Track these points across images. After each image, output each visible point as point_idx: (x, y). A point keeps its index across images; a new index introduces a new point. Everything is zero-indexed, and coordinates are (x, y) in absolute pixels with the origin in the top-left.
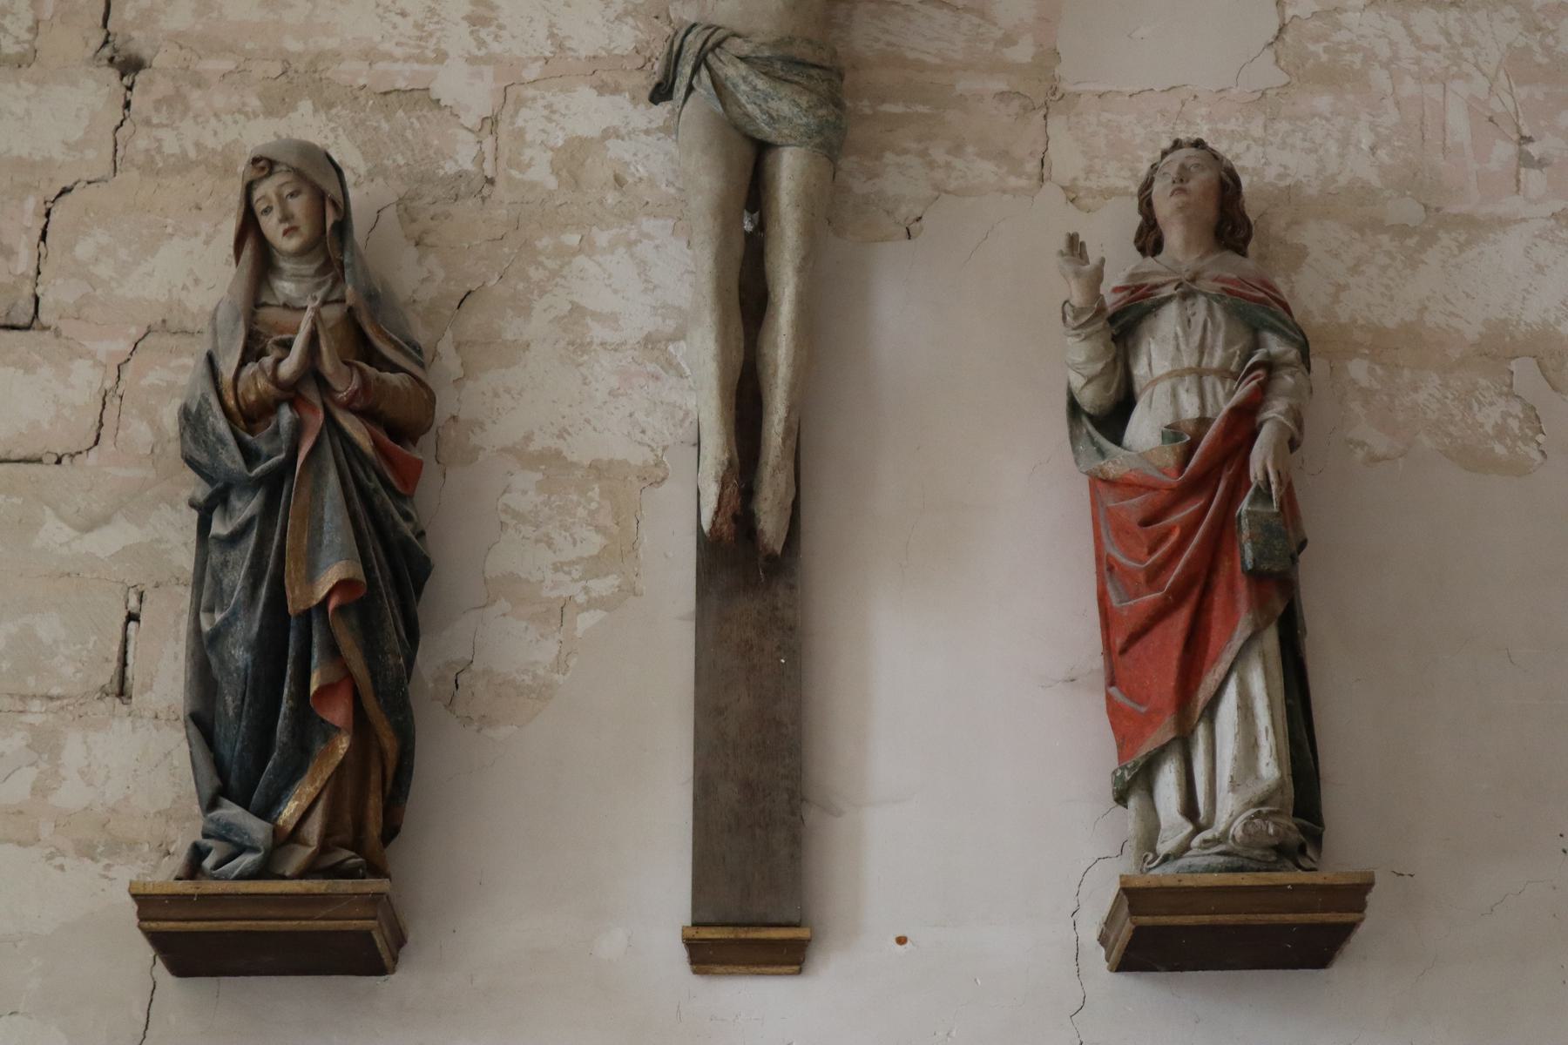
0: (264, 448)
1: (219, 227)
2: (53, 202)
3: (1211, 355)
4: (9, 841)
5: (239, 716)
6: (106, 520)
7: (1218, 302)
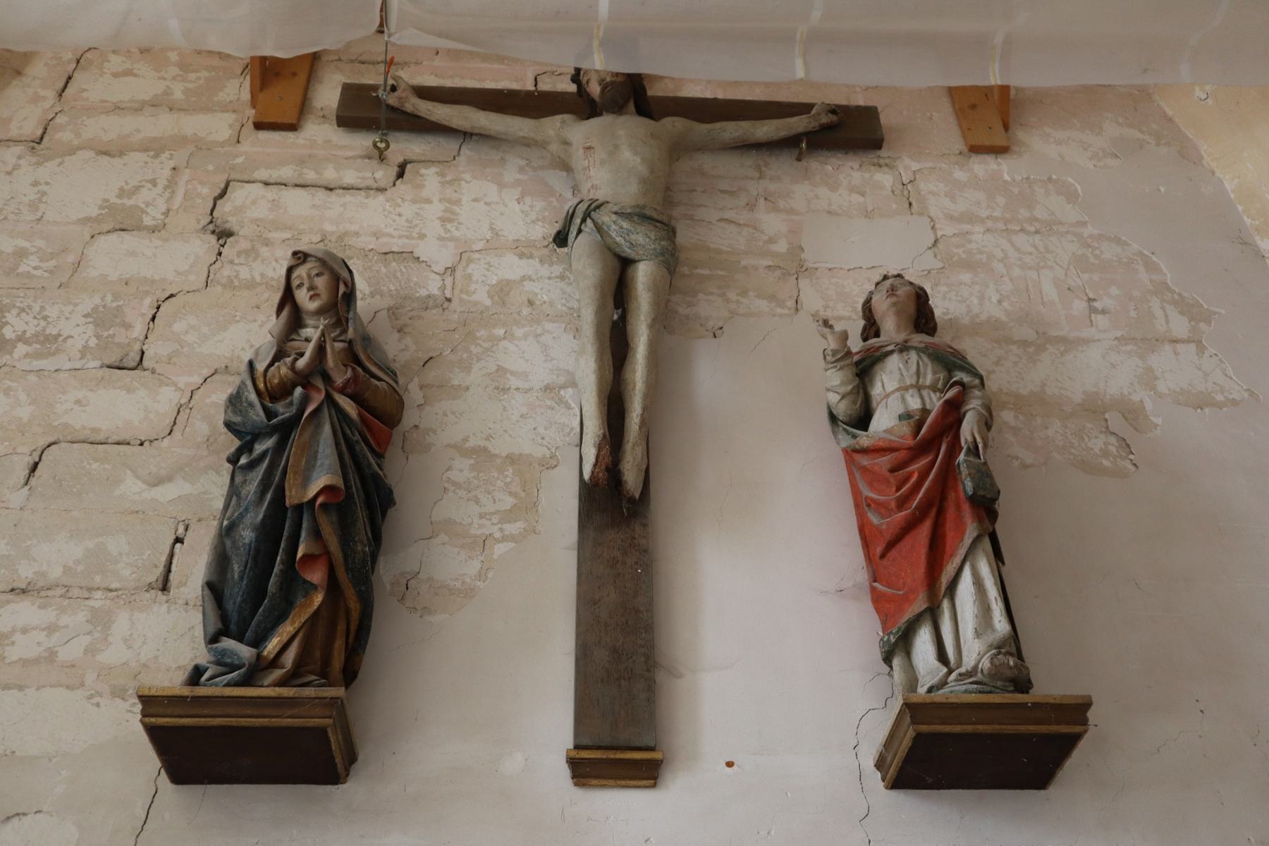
0: (281, 410)
1: (270, 318)
2: (163, 301)
3: (925, 378)
4: (61, 685)
5: (241, 578)
6: (169, 479)
7: (925, 353)
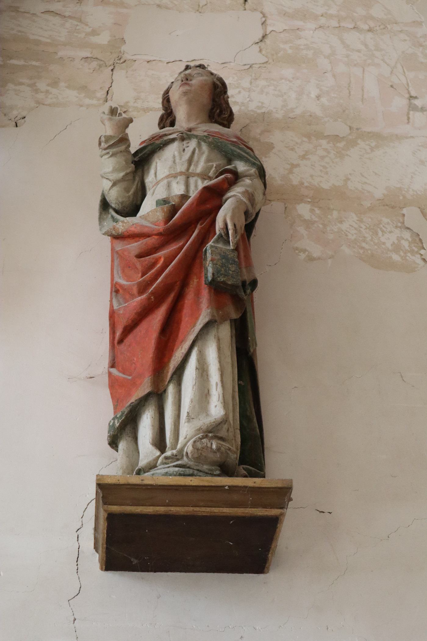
3: (196, 165)
7: (205, 142)
